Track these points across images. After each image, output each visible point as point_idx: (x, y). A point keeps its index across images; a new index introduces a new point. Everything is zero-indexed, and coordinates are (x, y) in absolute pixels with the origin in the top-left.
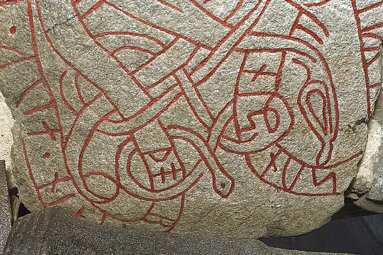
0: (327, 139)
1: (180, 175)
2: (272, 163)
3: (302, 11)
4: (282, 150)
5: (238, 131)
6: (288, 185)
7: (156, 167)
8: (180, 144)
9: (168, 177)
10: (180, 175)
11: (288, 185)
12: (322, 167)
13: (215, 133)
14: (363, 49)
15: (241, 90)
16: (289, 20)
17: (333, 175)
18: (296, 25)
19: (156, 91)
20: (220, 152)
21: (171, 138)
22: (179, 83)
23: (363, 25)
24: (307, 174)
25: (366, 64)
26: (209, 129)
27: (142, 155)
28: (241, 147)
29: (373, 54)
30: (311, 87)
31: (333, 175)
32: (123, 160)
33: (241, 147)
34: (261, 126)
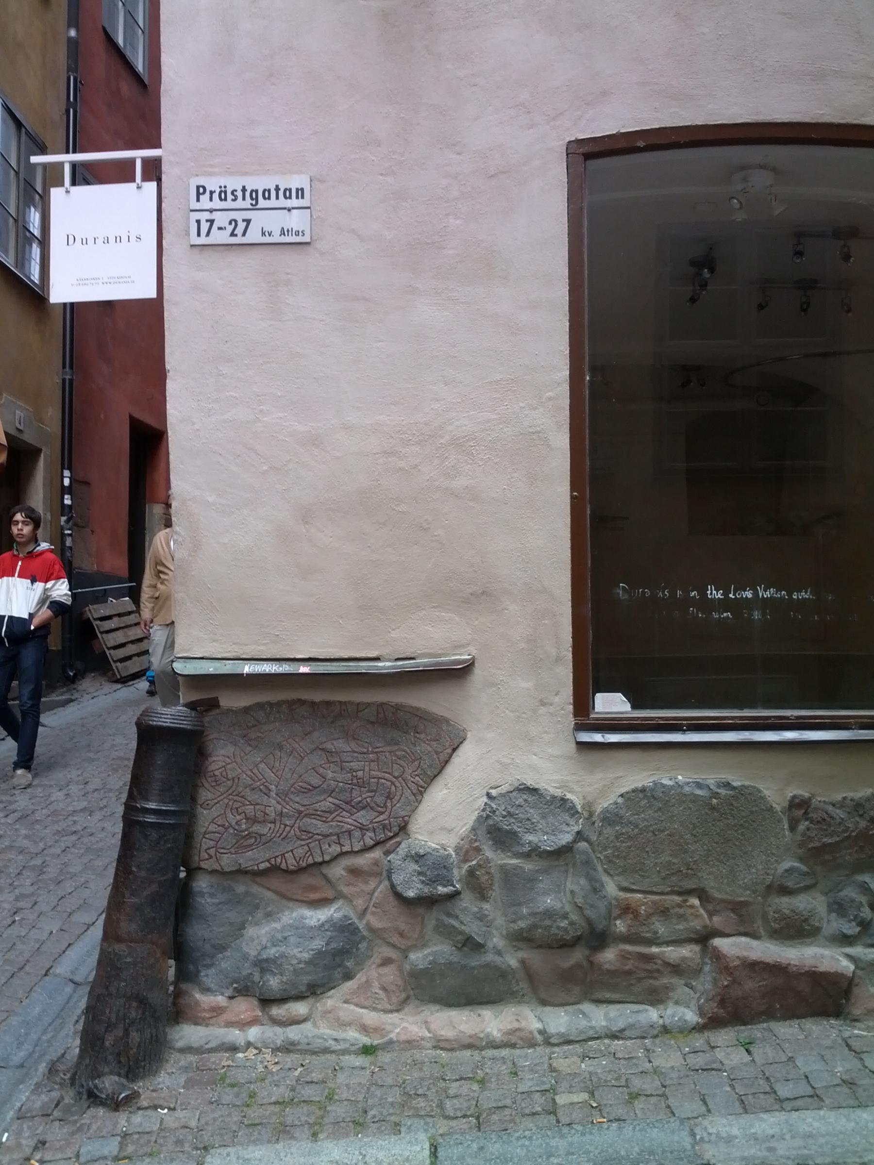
0: (233, 850)
1: (214, 784)
2: (219, 826)
3: (292, 827)
4: (226, 829)
5: (237, 809)
6: (207, 836)
7: (217, 773)
8: (229, 783)
9: (213, 779)
10: (214, 784)
11: (207, 836)
12: (216, 851)
13: (235, 798)
14: (275, 858)
15: (257, 807)
16: (288, 823)
17: (211, 857)
18: (286, 825)
19: (255, 771)
20: (226, 801)
21: (233, 779)
22: (260, 780)
23: (286, 855)
24: (212, 843)
25: (268, 861)
26: (237, 795)
27: (224, 767)
28: (228, 811)
29: (273, 863)
30: (258, 837)
31: (211, 857)
32: (221, 758)
33: (228, 811)
34: (238, 817)
